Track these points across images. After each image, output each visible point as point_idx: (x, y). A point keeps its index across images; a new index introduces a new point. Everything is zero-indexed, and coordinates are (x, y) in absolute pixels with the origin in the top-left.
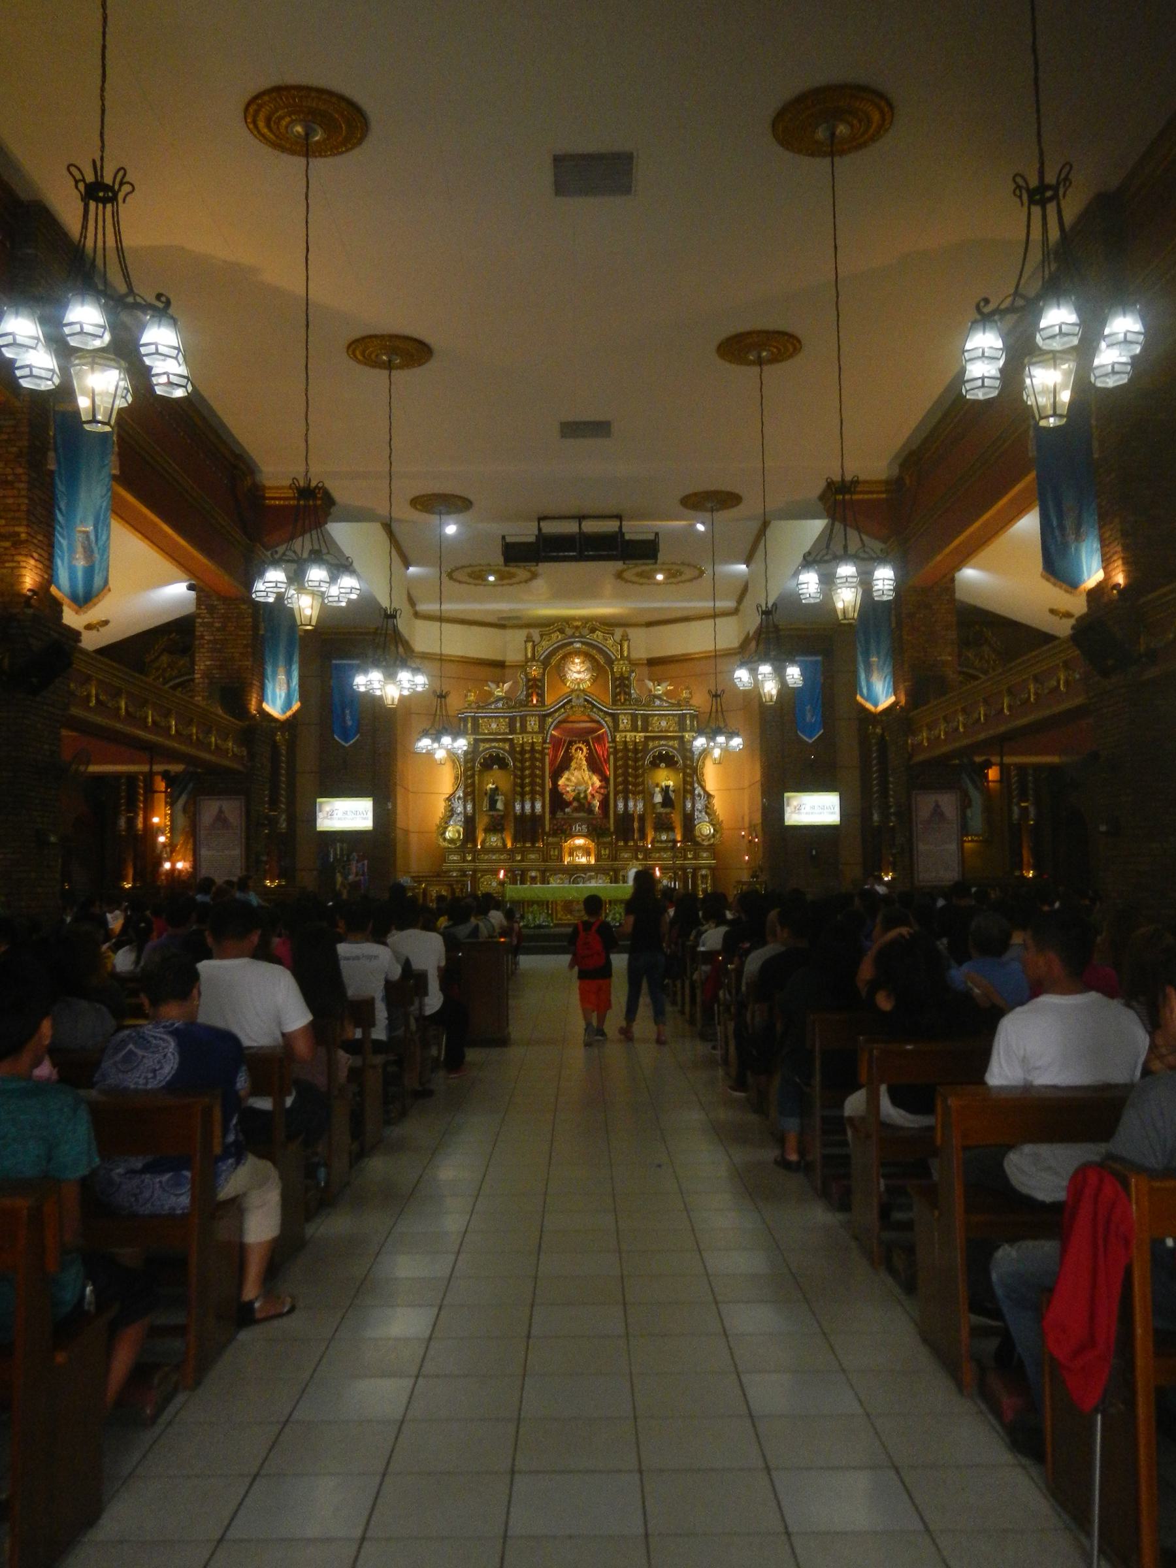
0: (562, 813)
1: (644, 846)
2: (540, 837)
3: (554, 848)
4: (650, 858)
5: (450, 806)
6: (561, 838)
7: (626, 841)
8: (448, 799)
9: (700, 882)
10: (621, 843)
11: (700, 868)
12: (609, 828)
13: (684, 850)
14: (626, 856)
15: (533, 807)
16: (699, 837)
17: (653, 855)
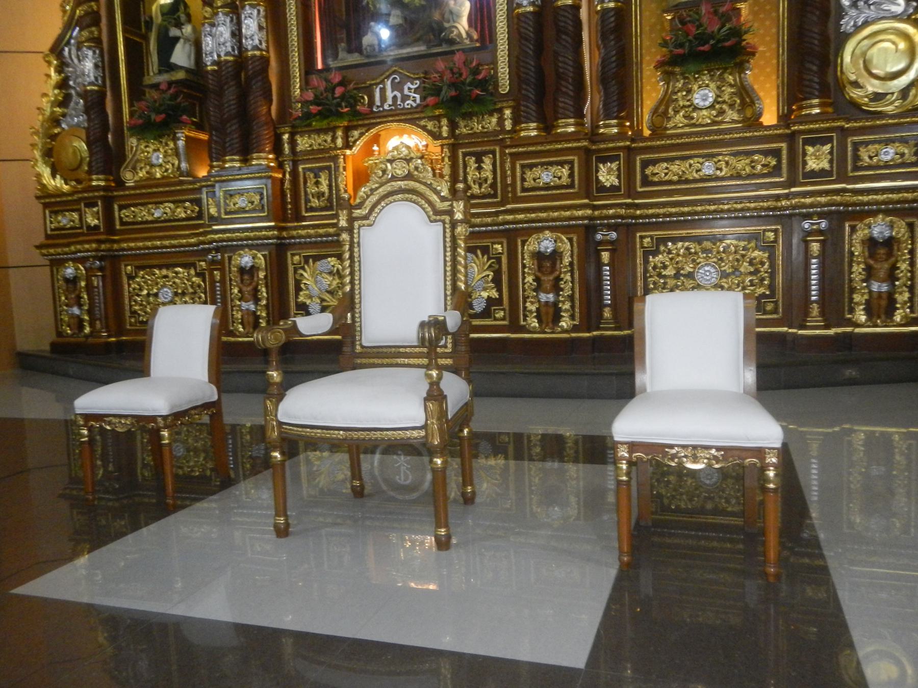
0: (356, 54)
1: (621, 136)
2: (266, 134)
3: (316, 172)
4: (646, 181)
5: (59, 70)
6: (334, 139)
7: (547, 126)
8: (57, 49)
9: (858, 269)
10: (531, 130)
11: (861, 214)
12: (488, 83)
13: (791, 138)
14: (546, 177)
15: (237, 34)
16: (856, 84)
17: (659, 171)
